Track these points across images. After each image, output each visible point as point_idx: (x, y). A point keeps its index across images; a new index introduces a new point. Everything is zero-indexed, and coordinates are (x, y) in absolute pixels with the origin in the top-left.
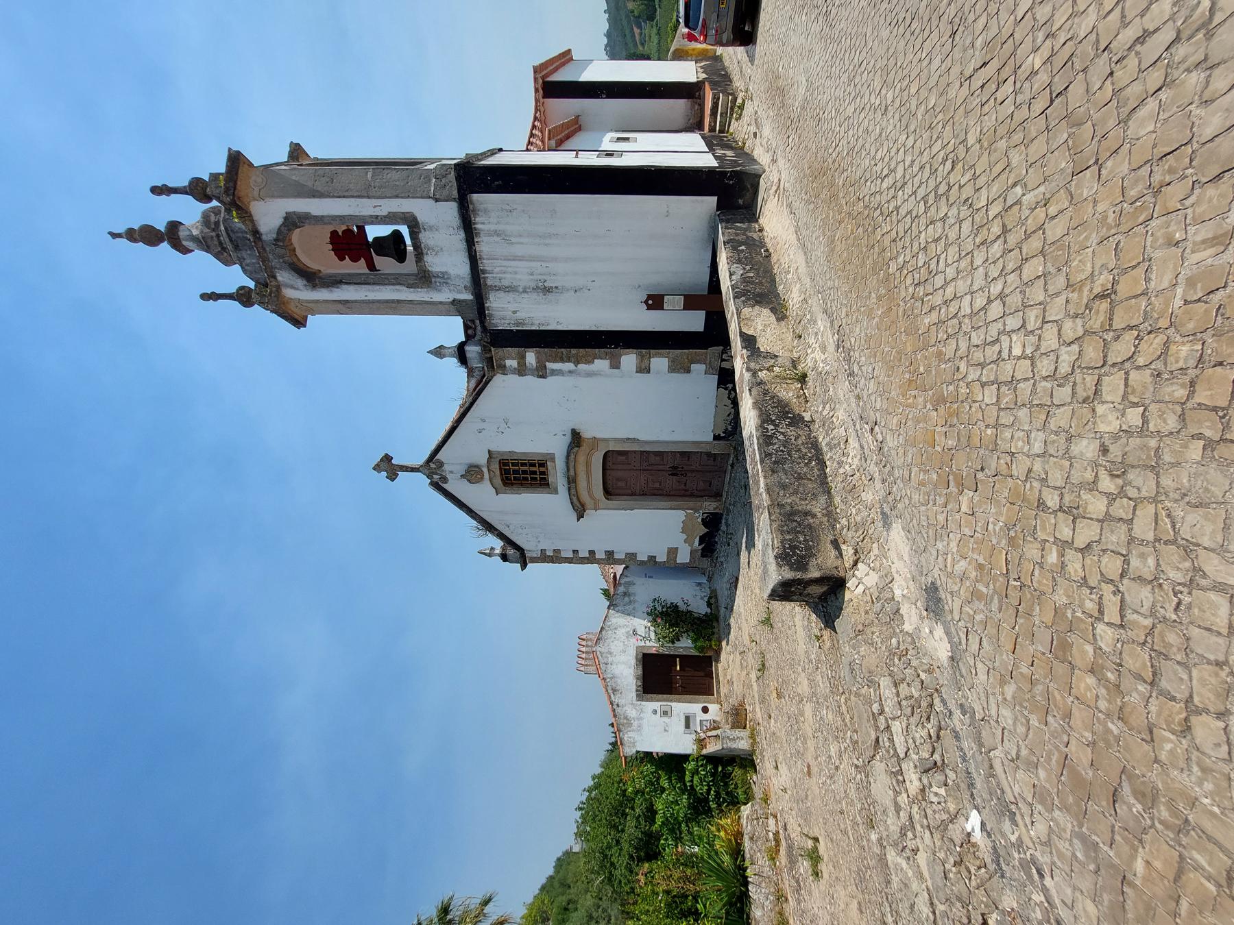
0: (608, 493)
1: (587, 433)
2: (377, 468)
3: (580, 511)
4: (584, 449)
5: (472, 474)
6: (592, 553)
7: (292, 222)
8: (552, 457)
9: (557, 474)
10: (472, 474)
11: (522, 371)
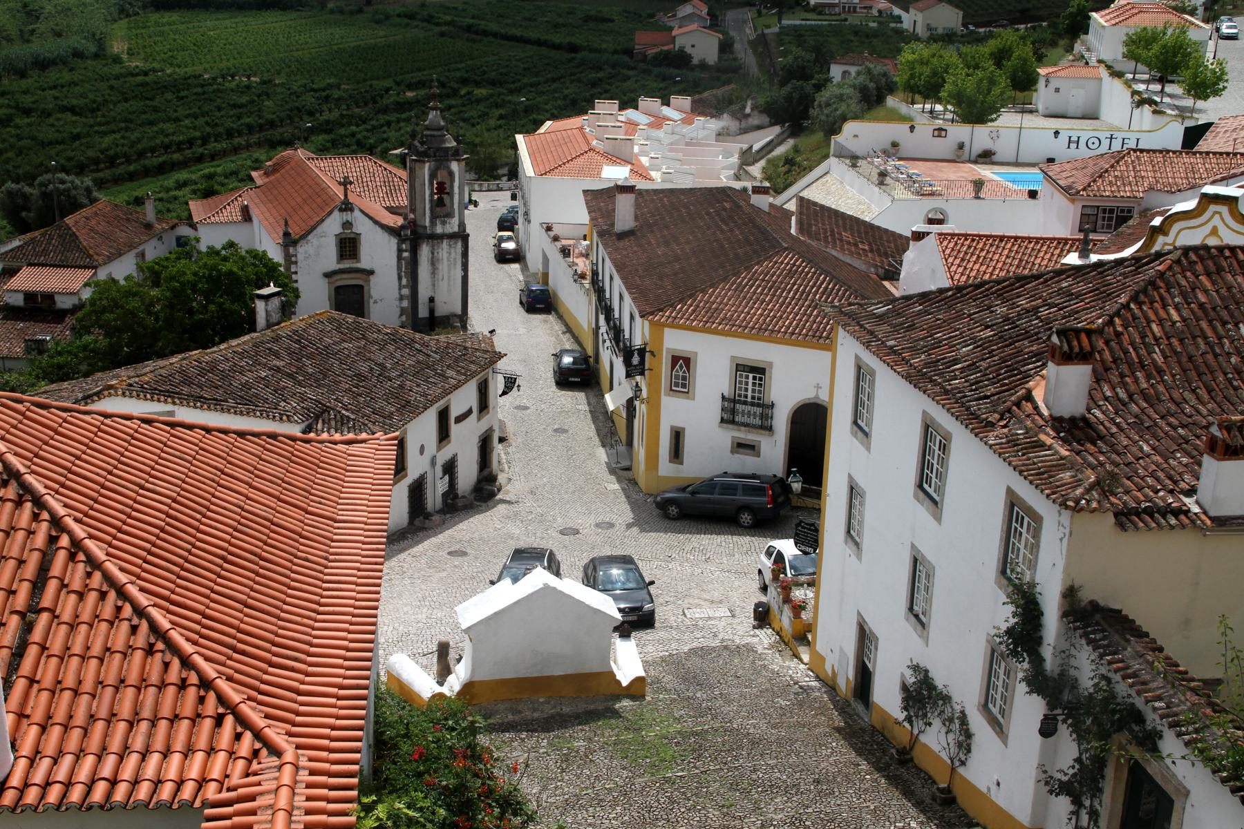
0: (338, 289)
1: (371, 277)
2: (346, 178)
3: (327, 275)
4: (364, 276)
5: (347, 225)
6: (296, 281)
7: (451, 174)
8: (358, 261)
9: (347, 264)
10: (347, 225)
11: (400, 251)
